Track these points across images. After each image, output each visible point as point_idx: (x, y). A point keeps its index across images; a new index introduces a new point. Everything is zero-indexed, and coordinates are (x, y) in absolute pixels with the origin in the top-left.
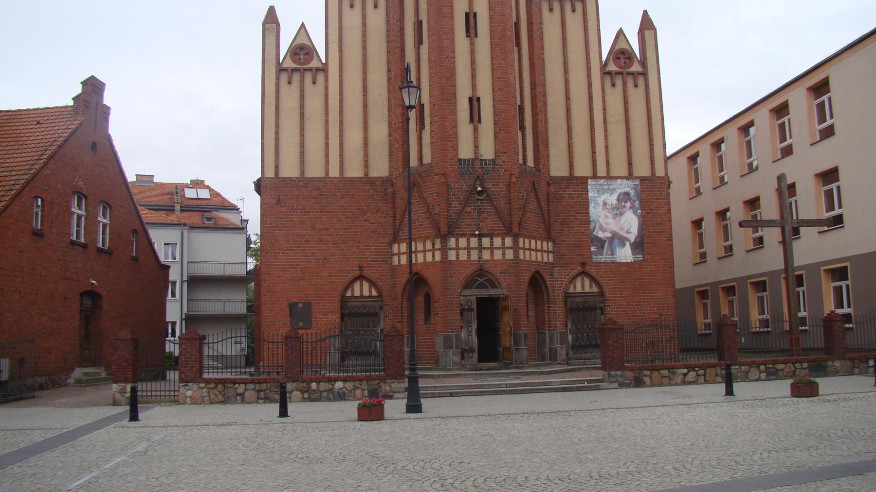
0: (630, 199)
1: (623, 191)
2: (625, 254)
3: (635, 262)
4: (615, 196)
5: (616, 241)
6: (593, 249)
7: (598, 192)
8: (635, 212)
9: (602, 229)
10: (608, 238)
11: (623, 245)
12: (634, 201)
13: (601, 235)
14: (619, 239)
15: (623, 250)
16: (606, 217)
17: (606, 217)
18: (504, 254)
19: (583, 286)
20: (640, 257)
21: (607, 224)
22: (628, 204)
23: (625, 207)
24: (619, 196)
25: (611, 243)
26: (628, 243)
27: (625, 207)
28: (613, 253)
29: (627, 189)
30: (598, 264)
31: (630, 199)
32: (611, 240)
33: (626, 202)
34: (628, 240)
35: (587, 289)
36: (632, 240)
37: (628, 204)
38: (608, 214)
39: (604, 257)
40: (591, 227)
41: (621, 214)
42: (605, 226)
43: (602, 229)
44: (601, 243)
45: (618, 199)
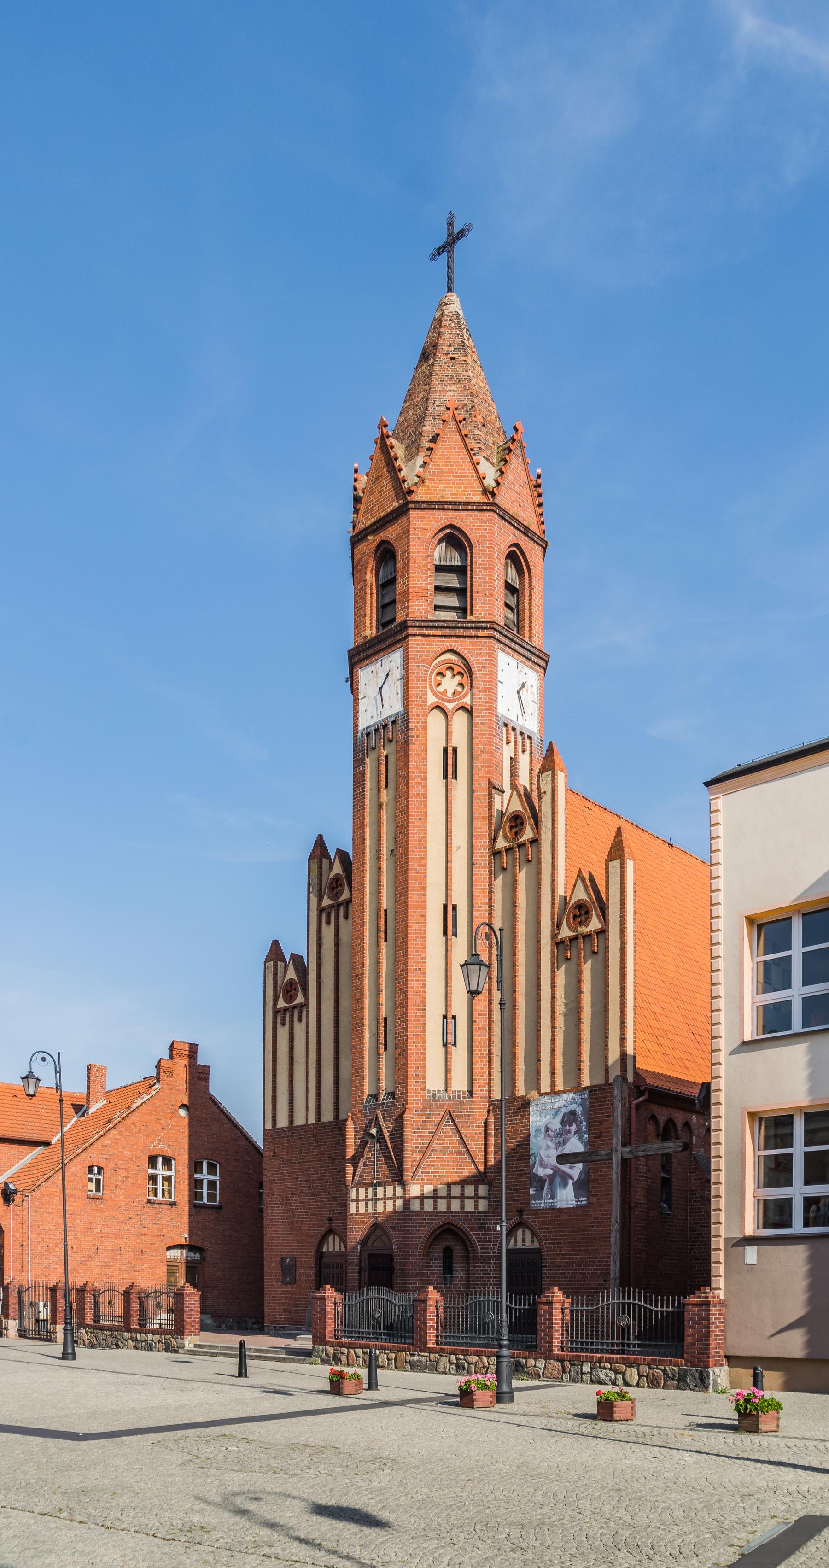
0: (575, 1120)
1: (568, 1110)
2: (567, 1197)
3: (578, 1207)
4: (559, 1118)
5: (558, 1180)
6: (532, 1191)
7: (540, 1116)
8: (581, 1138)
9: (543, 1165)
10: (548, 1176)
11: (565, 1185)
12: (581, 1123)
13: (541, 1172)
14: (561, 1176)
15: (564, 1192)
16: (548, 1147)
17: (548, 1147)
18: (435, 1205)
19: (523, 1240)
20: (583, 1201)
21: (548, 1157)
22: (574, 1128)
23: (569, 1132)
24: (563, 1117)
25: (551, 1184)
26: (570, 1182)
27: (569, 1132)
28: (553, 1197)
29: (573, 1107)
30: (536, 1211)
31: (575, 1120)
32: (552, 1178)
33: (571, 1125)
34: (571, 1178)
35: (528, 1244)
36: (576, 1178)
37: (574, 1128)
38: (550, 1144)
39: (543, 1203)
40: (531, 1162)
41: (565, 1142)
42: (545, 1159)
43: (543, 1165)
44: (540, 1182)
45: (563, 1123)
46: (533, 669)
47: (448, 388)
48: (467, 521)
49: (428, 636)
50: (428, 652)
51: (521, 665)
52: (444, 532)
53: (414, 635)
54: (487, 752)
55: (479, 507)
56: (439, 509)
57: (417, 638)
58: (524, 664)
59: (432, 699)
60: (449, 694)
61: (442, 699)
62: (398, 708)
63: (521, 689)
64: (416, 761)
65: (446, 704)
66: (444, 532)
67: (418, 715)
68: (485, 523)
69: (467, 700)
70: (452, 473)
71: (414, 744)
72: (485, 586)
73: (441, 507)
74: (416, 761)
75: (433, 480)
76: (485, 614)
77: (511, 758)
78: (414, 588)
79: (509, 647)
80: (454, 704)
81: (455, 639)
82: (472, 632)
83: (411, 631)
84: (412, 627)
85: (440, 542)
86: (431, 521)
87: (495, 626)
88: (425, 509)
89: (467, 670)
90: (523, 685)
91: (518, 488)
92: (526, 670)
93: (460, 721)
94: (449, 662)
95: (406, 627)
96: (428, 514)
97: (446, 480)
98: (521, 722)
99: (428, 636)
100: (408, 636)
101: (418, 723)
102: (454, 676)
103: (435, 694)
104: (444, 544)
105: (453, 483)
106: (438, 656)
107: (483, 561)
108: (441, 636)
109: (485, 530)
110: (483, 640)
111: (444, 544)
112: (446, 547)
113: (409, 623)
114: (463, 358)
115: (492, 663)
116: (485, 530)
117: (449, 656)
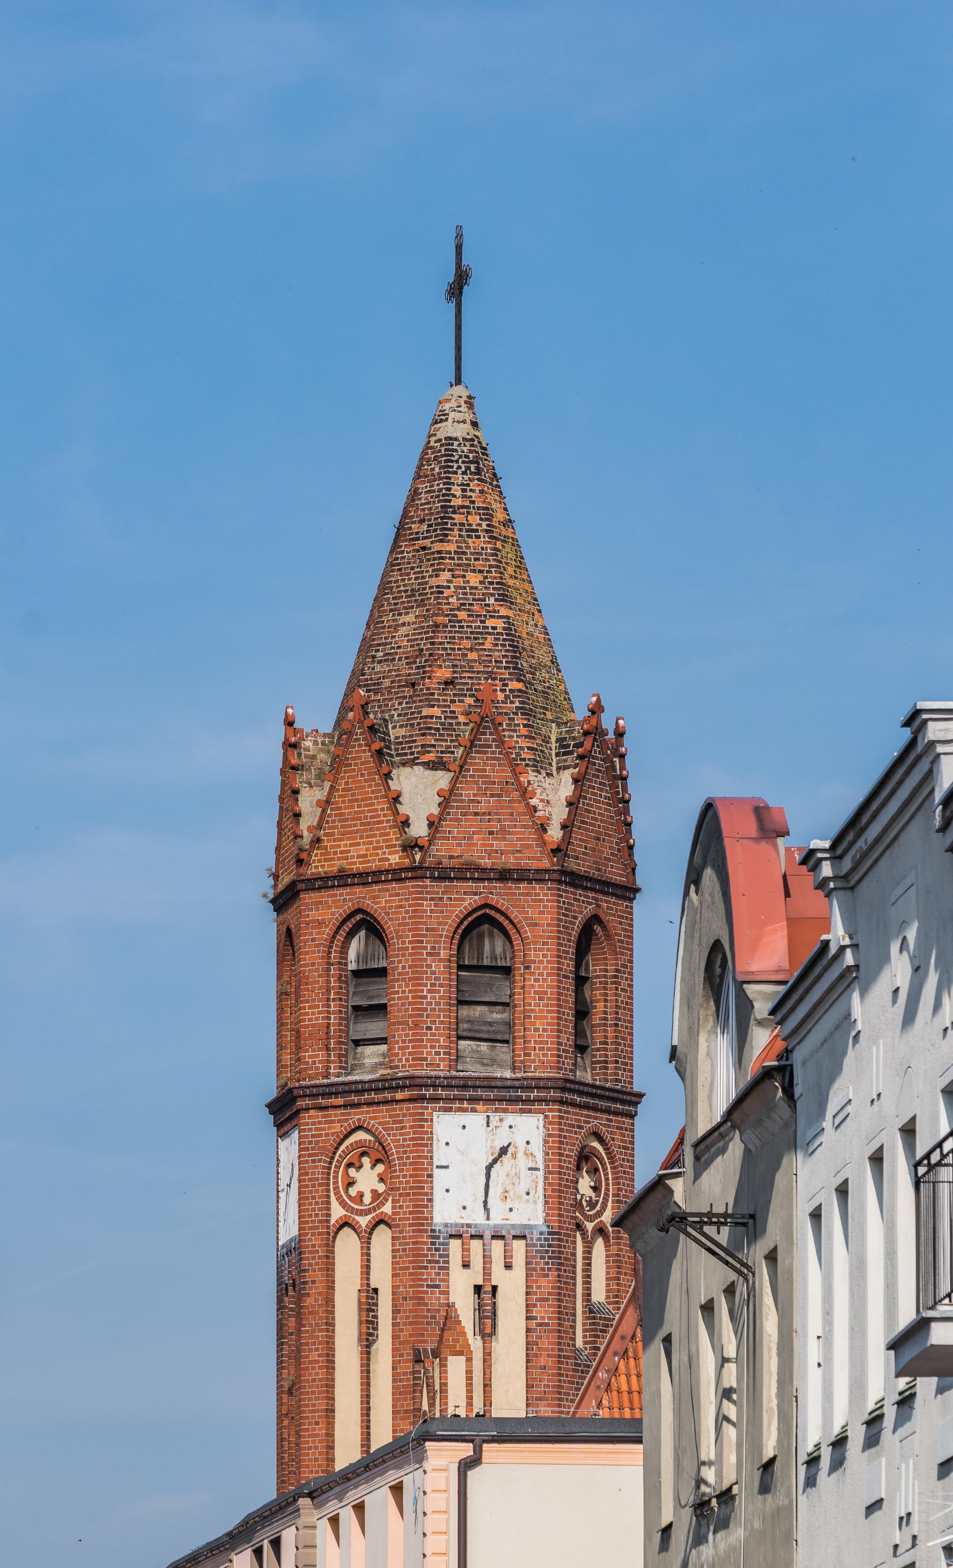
46: (530, 1111)
47: (402, 619)
48: (383, 902)
49: (326, 1108)
50: (327, 1135)
51: (495, 1118)
52: (353, 921)
53: (307, 1109)
54: (411, 1299)
55: (397, 875)
56: (339, 886)
57: (312, 1113)
58: (505, 1111)
59: (337, 1212)
60: (367, 1199)
61: (352, 1210)
62: (295, 1232)
63: (495, 1161)
64: (310, 1325)
65: (357, 1218)
66: (353, 921)
67: (314, 1246)
68: (407, 900)
69: (387, 1209)
70: (359, 819)
71: (308, 1295)
72: (407, 1010)
73: (342, 883)
74: (310, 1325)
75: (333, 834)
76: (407, 1060)
77: (478, 1289)
78: (307, 1026)
79: (461, 1100)
80: (370, 1216)
81: (365, 1109)
82: (388, 1095)
83: (300, 1103)
84: (301, 1096)
85: (351, 934)
86: (329, 908)
87: (418, 1081)
88: (320, 888)
89: (381, 1156)
90: (504, 1151)
91: (486, 803)
92: (510, 1119)
93: (382, 1240)
94: (359, 1144)
95: (294, 1099)
96: (324, 896)
97: (350, 833)
98: (497, 1218)
99: (326, 1108)
100: (298, 1112)
101: (314, 1258)
102: (373, 1166)
103: (343, 1204)
104: (362, 933)
105: (361, 837)
106: (343, 1141)
107: (404, 967)
108: (345, 1106)
109: (407, 912)
110: (405, 1106)
111: (362, 933)
112: (367, 937)
113: (295, 1092)
114: (437, 547)
115: (423, 1140)
116: (407, 912)
117: (360, 1136)
